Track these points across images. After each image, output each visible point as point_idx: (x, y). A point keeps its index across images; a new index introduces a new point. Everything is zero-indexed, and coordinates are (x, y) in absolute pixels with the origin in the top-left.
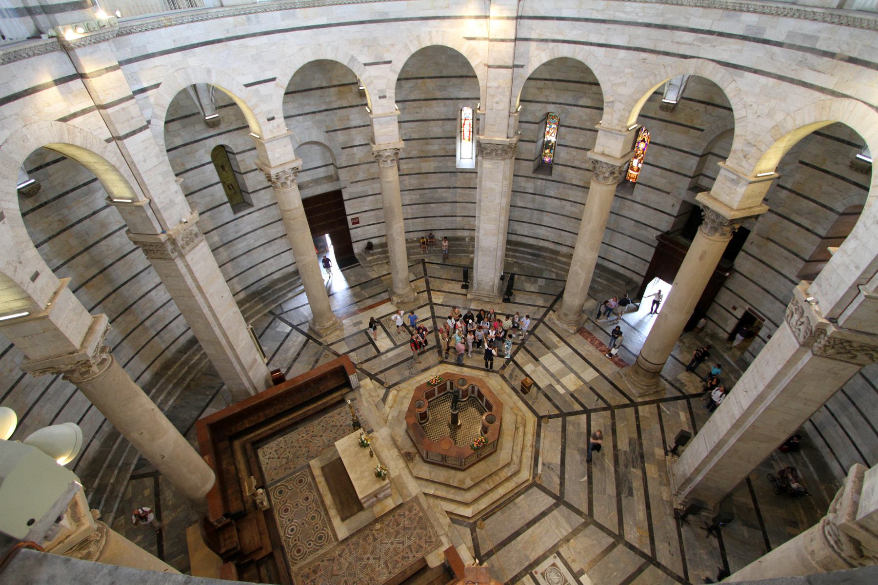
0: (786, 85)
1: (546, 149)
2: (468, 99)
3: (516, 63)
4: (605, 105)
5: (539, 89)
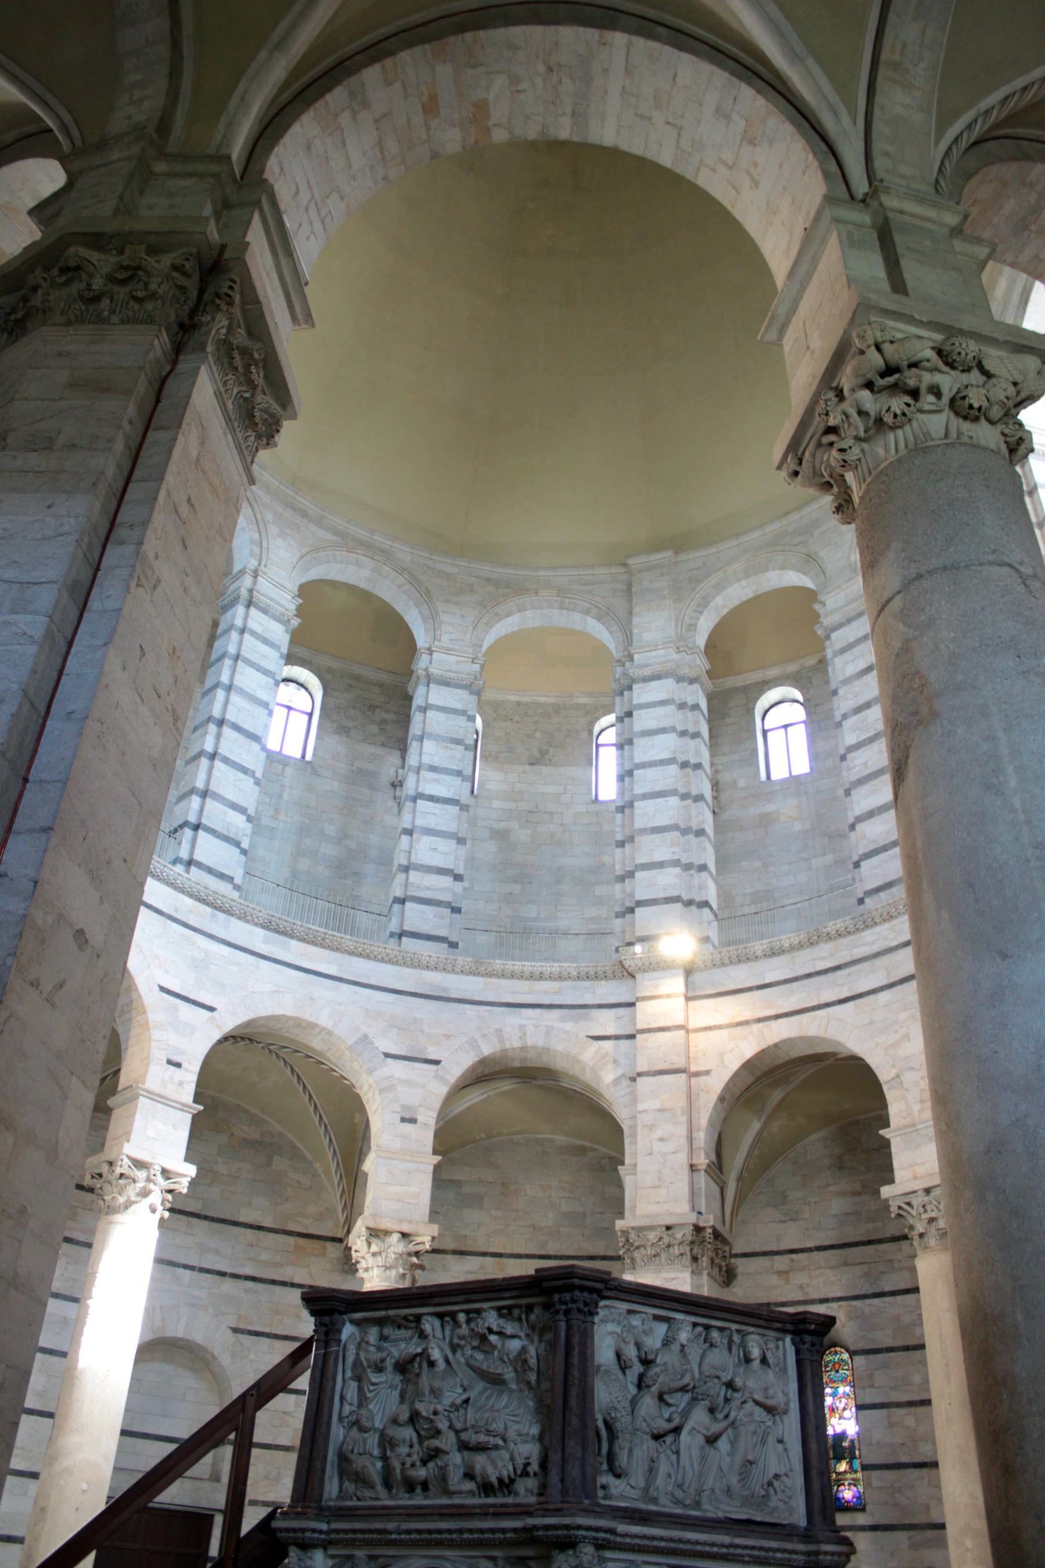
1: (839, 1459)
5: (780, 1273)
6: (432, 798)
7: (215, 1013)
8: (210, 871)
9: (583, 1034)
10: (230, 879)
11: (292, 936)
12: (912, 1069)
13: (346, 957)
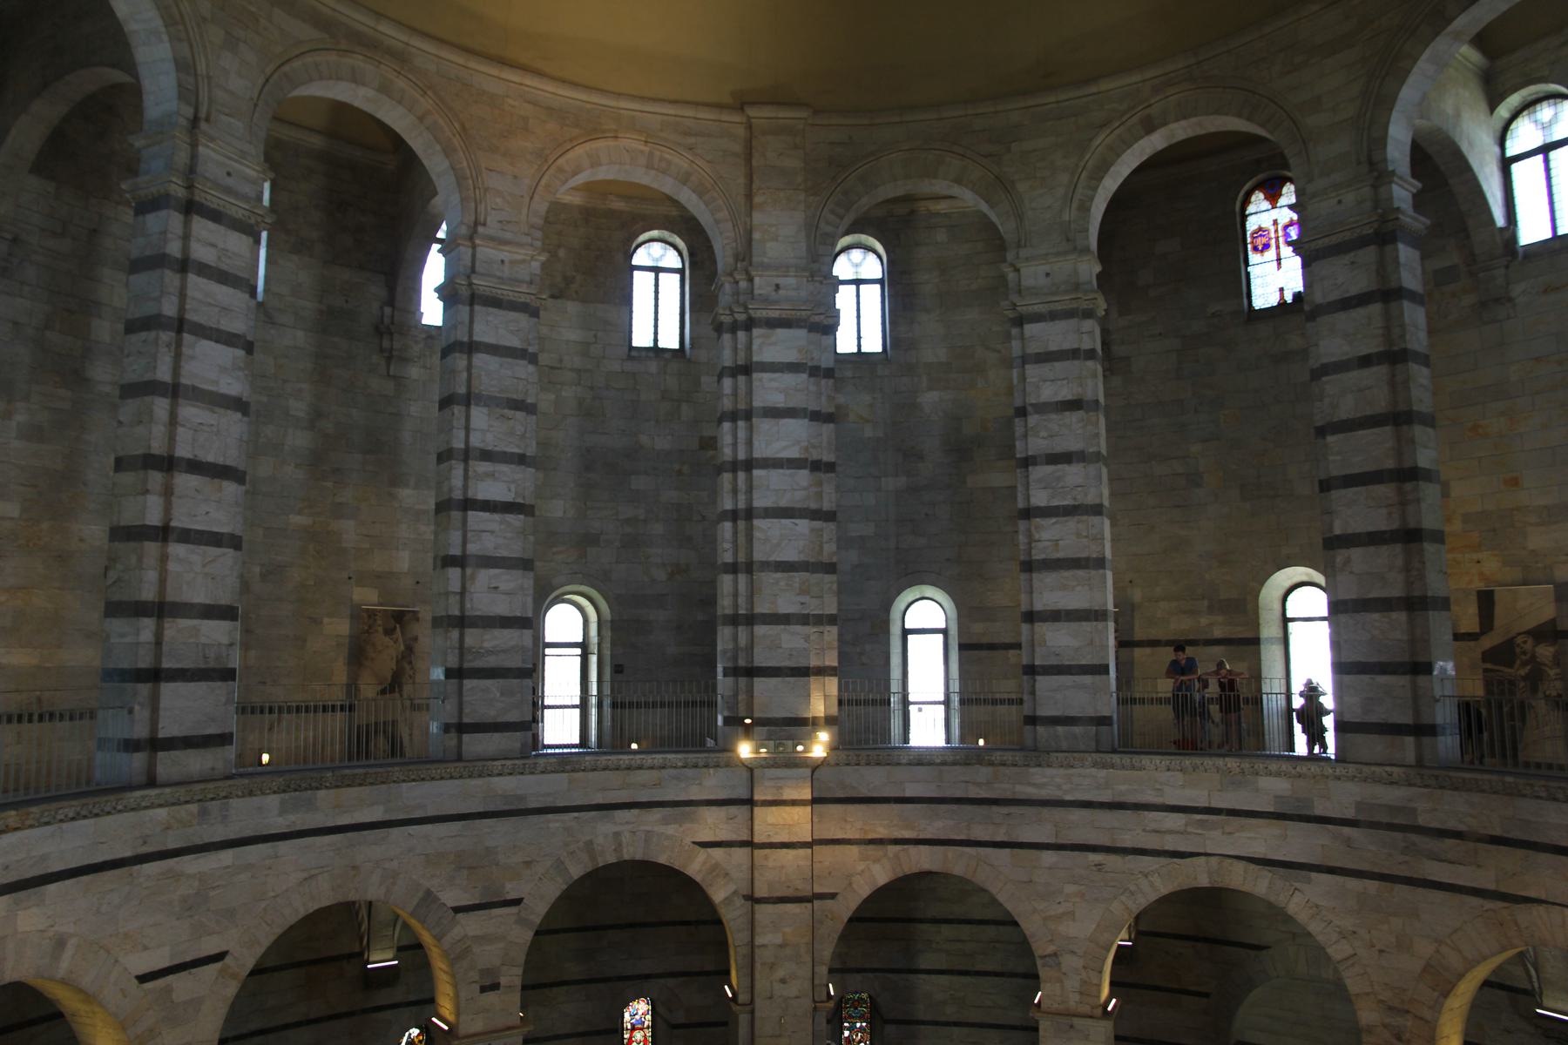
0: (1402, 891)
2: (647, 977)
3: (818, 889)
4: (1039, 962)
6: (488, 506)
7: (228, 960)
9: (688, 840)
12: (1073, 952)
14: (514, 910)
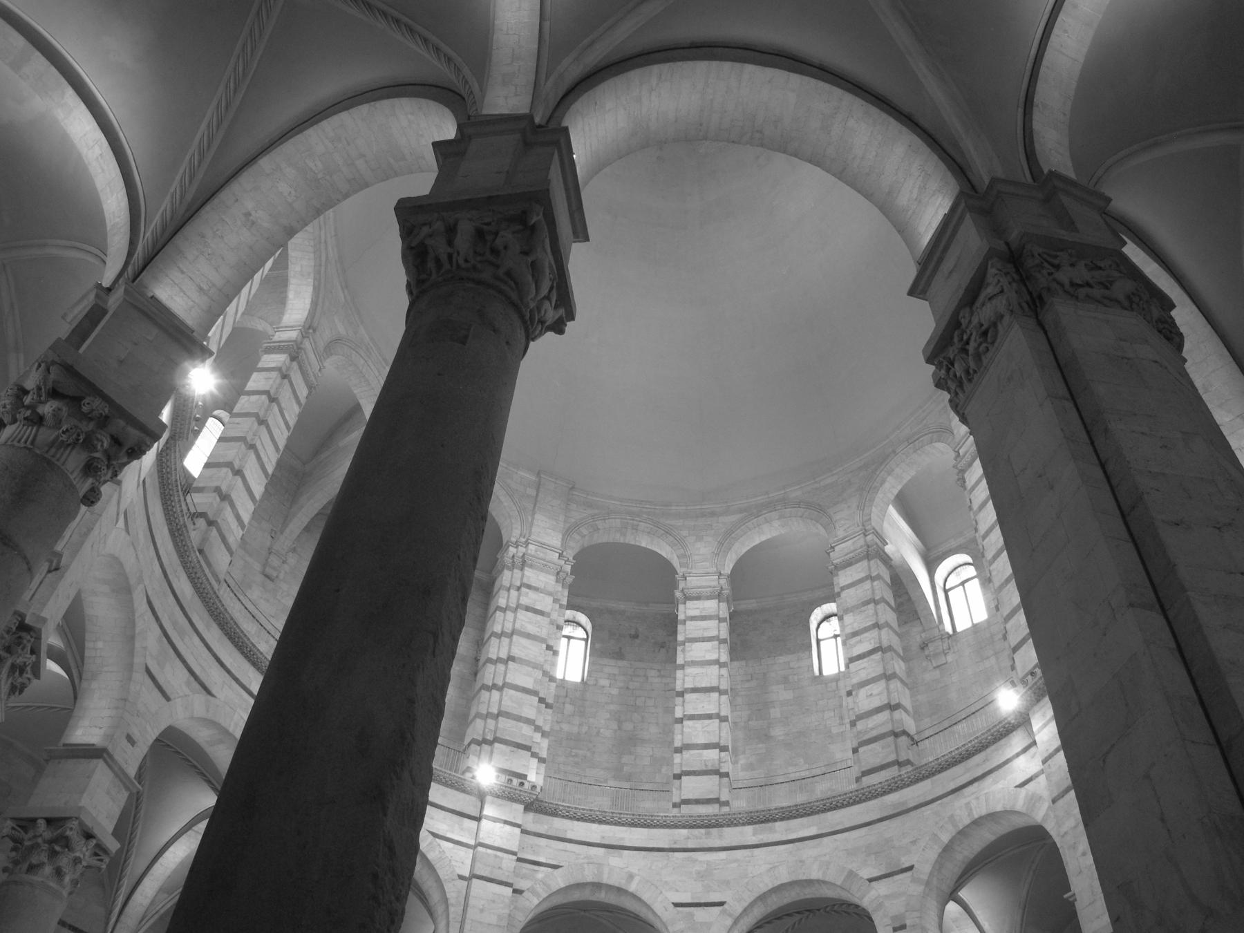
8: (698, 802)
10: (716, 801)
11: (775, 821)
13: (822, 816)
14: (908, 874)
